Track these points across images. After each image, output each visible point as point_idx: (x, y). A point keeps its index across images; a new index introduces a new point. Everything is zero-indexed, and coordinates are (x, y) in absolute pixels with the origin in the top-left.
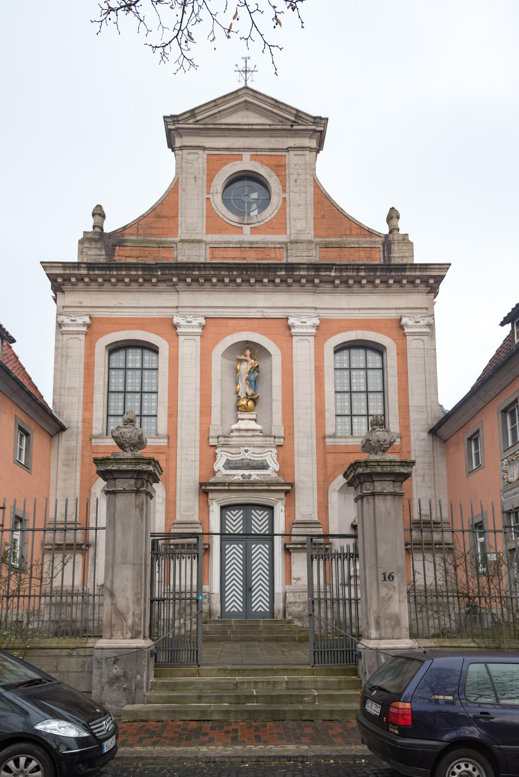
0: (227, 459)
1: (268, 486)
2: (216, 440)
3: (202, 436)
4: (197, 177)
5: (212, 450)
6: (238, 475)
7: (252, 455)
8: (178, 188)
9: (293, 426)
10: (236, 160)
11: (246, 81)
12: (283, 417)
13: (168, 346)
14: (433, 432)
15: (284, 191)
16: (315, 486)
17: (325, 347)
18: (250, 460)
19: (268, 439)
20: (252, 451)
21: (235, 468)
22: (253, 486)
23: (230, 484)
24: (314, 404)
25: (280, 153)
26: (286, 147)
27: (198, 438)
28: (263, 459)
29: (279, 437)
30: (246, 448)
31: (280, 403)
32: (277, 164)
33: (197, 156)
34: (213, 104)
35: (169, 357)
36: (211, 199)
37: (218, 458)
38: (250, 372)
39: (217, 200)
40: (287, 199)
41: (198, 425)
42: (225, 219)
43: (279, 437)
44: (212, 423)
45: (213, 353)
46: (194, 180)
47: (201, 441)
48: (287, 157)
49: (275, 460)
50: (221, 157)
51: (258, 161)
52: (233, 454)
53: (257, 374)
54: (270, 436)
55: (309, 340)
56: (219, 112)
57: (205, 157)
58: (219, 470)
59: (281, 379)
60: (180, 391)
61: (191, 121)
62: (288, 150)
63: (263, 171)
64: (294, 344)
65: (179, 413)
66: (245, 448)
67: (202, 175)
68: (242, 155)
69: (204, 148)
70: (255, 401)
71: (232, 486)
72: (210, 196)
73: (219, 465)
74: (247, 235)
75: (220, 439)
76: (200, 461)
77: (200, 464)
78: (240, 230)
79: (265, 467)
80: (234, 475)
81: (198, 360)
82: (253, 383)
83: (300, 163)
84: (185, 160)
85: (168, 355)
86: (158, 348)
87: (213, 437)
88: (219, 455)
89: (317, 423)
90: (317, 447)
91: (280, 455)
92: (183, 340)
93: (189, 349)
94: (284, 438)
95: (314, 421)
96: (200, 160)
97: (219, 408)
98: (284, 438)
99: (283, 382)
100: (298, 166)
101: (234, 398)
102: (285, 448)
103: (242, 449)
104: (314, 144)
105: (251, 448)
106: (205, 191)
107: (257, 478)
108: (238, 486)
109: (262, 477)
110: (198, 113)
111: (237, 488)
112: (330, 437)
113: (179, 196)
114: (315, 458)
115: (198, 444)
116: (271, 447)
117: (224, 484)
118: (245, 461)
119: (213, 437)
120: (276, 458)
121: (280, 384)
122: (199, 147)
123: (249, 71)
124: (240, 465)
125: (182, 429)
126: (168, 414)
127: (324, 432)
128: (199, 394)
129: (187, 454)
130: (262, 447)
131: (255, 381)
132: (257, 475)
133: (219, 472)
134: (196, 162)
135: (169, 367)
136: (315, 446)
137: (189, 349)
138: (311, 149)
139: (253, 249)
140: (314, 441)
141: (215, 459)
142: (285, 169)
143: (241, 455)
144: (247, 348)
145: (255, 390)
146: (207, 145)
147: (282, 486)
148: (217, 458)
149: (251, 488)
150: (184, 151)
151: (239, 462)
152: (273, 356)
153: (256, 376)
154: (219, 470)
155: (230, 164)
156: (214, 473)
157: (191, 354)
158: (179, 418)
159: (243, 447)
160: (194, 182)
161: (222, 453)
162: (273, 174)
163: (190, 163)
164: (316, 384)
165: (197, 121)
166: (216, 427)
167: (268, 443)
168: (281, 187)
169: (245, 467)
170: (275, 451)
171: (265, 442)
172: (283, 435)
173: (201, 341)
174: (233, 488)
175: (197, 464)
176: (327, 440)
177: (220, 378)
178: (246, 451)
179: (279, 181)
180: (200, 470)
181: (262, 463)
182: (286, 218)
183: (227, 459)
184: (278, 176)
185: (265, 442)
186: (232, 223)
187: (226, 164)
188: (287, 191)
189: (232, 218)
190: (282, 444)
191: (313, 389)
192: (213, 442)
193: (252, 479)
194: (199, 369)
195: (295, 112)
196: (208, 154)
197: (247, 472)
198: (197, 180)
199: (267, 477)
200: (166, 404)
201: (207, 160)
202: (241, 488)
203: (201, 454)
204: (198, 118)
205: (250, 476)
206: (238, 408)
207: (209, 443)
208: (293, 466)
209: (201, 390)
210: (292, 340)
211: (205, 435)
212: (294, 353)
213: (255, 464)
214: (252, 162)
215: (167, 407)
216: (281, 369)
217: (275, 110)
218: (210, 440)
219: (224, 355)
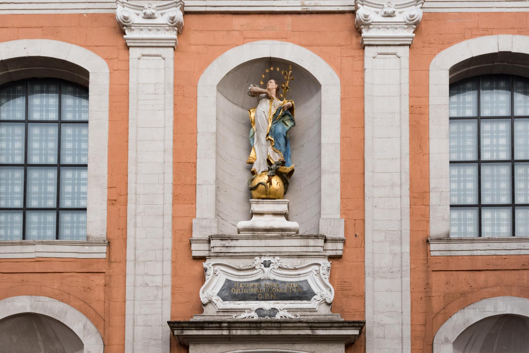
0: (228, 281)
1: (312, 328)
2: (205, 246)
3: (176, 240)
5: (197, 267)
6: (248, 310)
7: (278, 271)
9: (364, 220)
12: (342, 203)
13: (107, 70)
16: (407, 333)
17: (431, 67)
18: (275, 280)
19: (311, 242)
20: (279, 264)
21: (244, 298)
22: (279, 328)
23: (231, 325)
24: (406, 177)
27: (169, 242)
28: (302, 279)
29: (335, 240)
30: (267, 259)
31: (337, 177)
35: (111, 90)
37: (208, 279)
38: (277, 118)
41: (168, 219)
43: (335, 240)
44: (198, 216)
45: (200, 84)
47: (174, 250)
49: (327, 282)
52: (240, 270)
53: (290, 124)
54: (317, 237)
55: (399, 55)
58: (210, 302)
59: (339, 132)
60: (131, 154)
64: (368, 62)
65: (131, 196)
66: (263, 259)
70: (287, 178)
71: (236, 328)
73: (211, 290)
75: (213, 243)
76: (173, 287)
77: (173, 294)
79: (303, 294)
80: (242, 311)
81: (170, 95)
82: (282, 141)
85: (108, 86)
86: (86, 73)
87: (198, 241)
88: (210, 272)
89: (412, 215)
90: (413, 260)
91: (336, 276)
92: (139, 55)
93: (151, 74)
94: (343, 241)
95: (407, 210)
97: (213, 188)
98: (343, 241)
99: (342, 138)
102: (345, 259)
103: (258, 261)
105: (277, 258)
107: (289, 315)
108: (249, 328)
109: (298, 314)
111: (246, 332)
112: (439, 240)
114: (407, 280)
115: (168, 255)
116: (319, 256)
117: (219, 325)
118: (263, 283)
119: (198, 241)
120: (327, 277)
121: (338, 141)
124: (254, 291)
125: (135, 227)
126: (108, 200)
127: (427, 231)
128: (171, 160)
129: (146, 274)
130: (299, 256)
131: (285, 138)
132: (289, 310)
133: (210, 306)
135: (110, 110)
136: (407, 258)
137: (151, 74)
140: (407, 248)
141: (203, 280)
143: (255, 272)
144: (271, 76)
145: (286, 154)
147: (340, 328)
148: (207, 277)
149: (275, 332)
151: (251, 285)
152: (322, 87)
153: (287, 128)
154: (210, 302)
156: (201, 307)
157: (156, 84)
158: (131, 207)
159: (260, 256)
161: (217, 267)
164: (411, 139)
166: (205, 223)
167: (311, 249)
169: (263, 294)
170: (326, 263)
171: (305, 249)
172: (342, 236)
173: (176, 59)
174: (239, 332)
175: (168, 292)
176: (433, 246)
177: (214, 130)
178: (267, 264)
180: (173, 304)
181: (299, 287)
183: (228, 281)
185: (305, 249)
190: (340, 253)
191: (406, 149)
192: (199, 250)
193: (278, 317)
194: (170, 113)
197: (267, 305)
199: (308, 313)
200: (104, 181)
202: (254, 332)
203: (175, 275)
205: (274, 310)
206: (252, 190)
207: (191, 251)
208: (362, 297)
209: (176, 152)
210: (363, 55)
211: (183, 237)
212: (367, 79)
213: (284, 289)
215: (106, 186)
216: (339, 112)
218: (194, 246)
219: (222, 86)
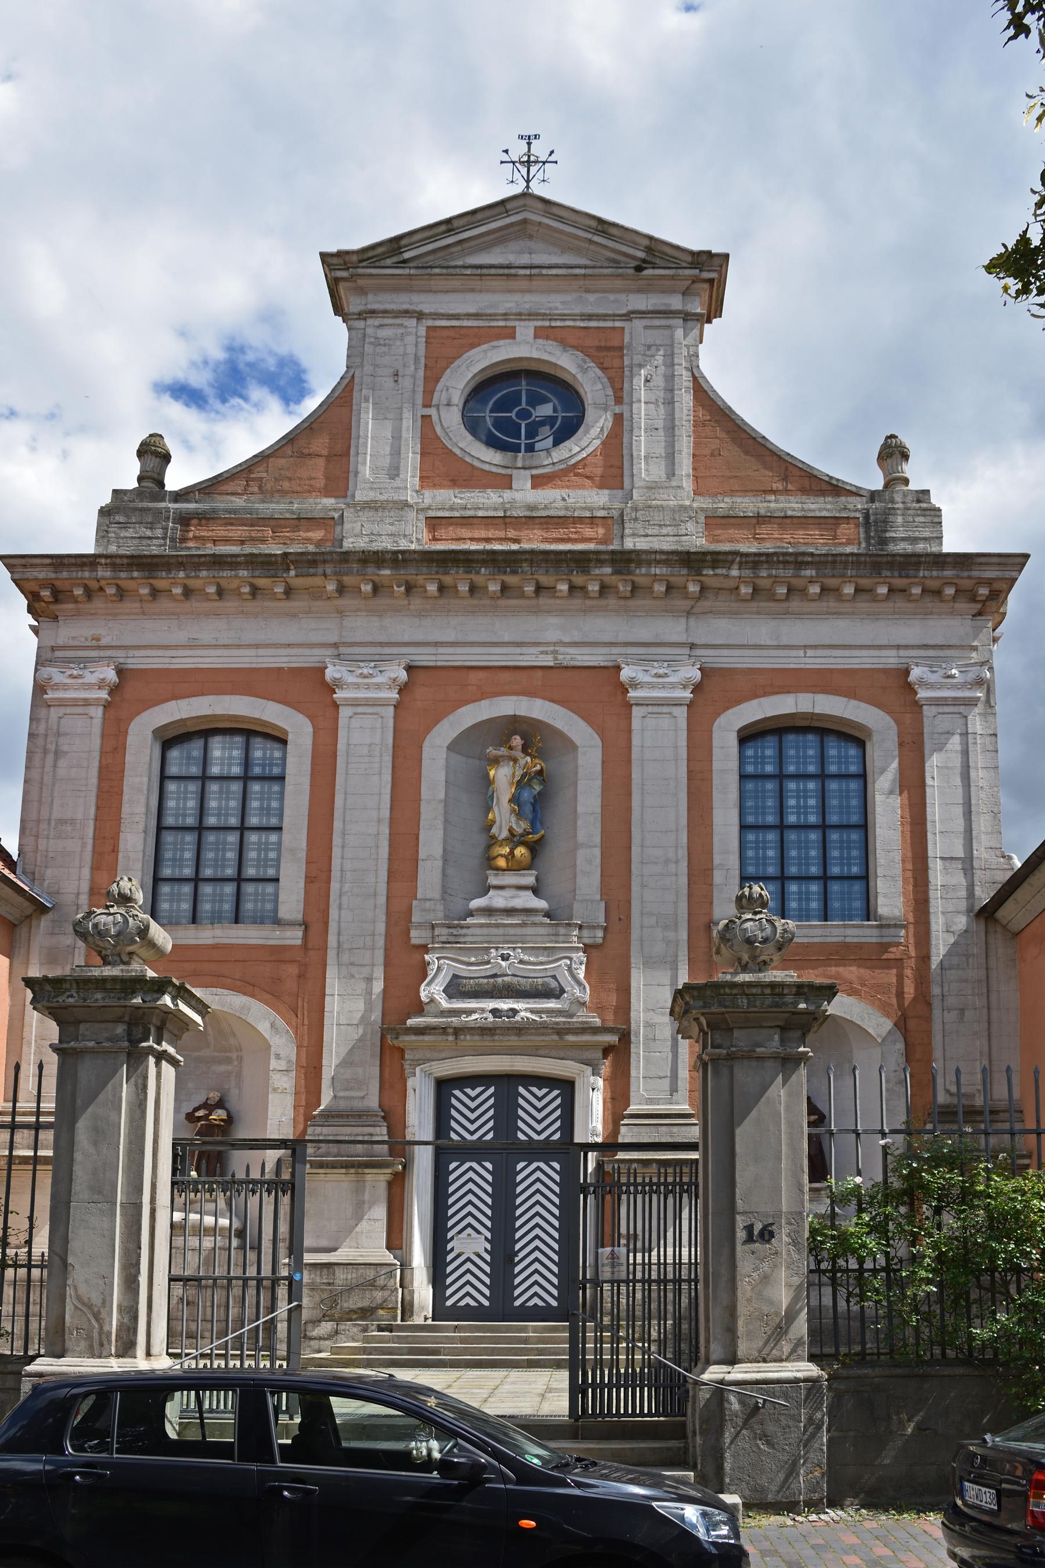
4: (400, 374)
8: (351, 396)
10: (498, 337)
11: (528, 181)
14: (987, 914)
15: (619, 400)
17: (715, 728)
25: (609, 324)
26: (624, 312)
32: (603, 344)
33: (401, 331)
34: (443, 228)
36: (435, 418)
39: (450, 420)
40: (626, 415)
42: (468, 459)
46: (392, 379)
48: (627, 331)
50: (463, 332)
51: (555, 340)
56: (460, 242)
57: (422, 331)
61: (388, 262)
62: (628, 316)
63: (566, 362)
67: (412, 368)
68: (515, 327)
69: (420, 316)
70: (535, 848)
72: (432, 412)
74: (524, 494)
78: (505, 482)
83: (658, 342)
84: (372, 340)
96: (410, 339)
100: (653, 348)
101: (481, 840)
104: (698, 307)
106: (419, 399)
110: (406, 246)
113: (354, 413)
122: (407, 312)
123: (536, 162)
134: (398, 343)
138: (687, 317)
139: (537, 521)
142: (622, 357)
146: (426, 309)
150: (370, 322)
155: (485, 347)
160: (392, 384)
162: (592, 364)
163: (385, 345)
165: (404, 261)
168: (610, 392)
179: (605, 380)
182: (622, 456)
184: (603, 369)
186: (486, 467)
187: (472, 346)
188: (626, 399)
189: (489, 457)
195: (646, 242)
196: (428, 327)
198: (400, 380)
201: (427, 337)
204: (407, 255)
214: (540, 341)
217: (596, 239)
